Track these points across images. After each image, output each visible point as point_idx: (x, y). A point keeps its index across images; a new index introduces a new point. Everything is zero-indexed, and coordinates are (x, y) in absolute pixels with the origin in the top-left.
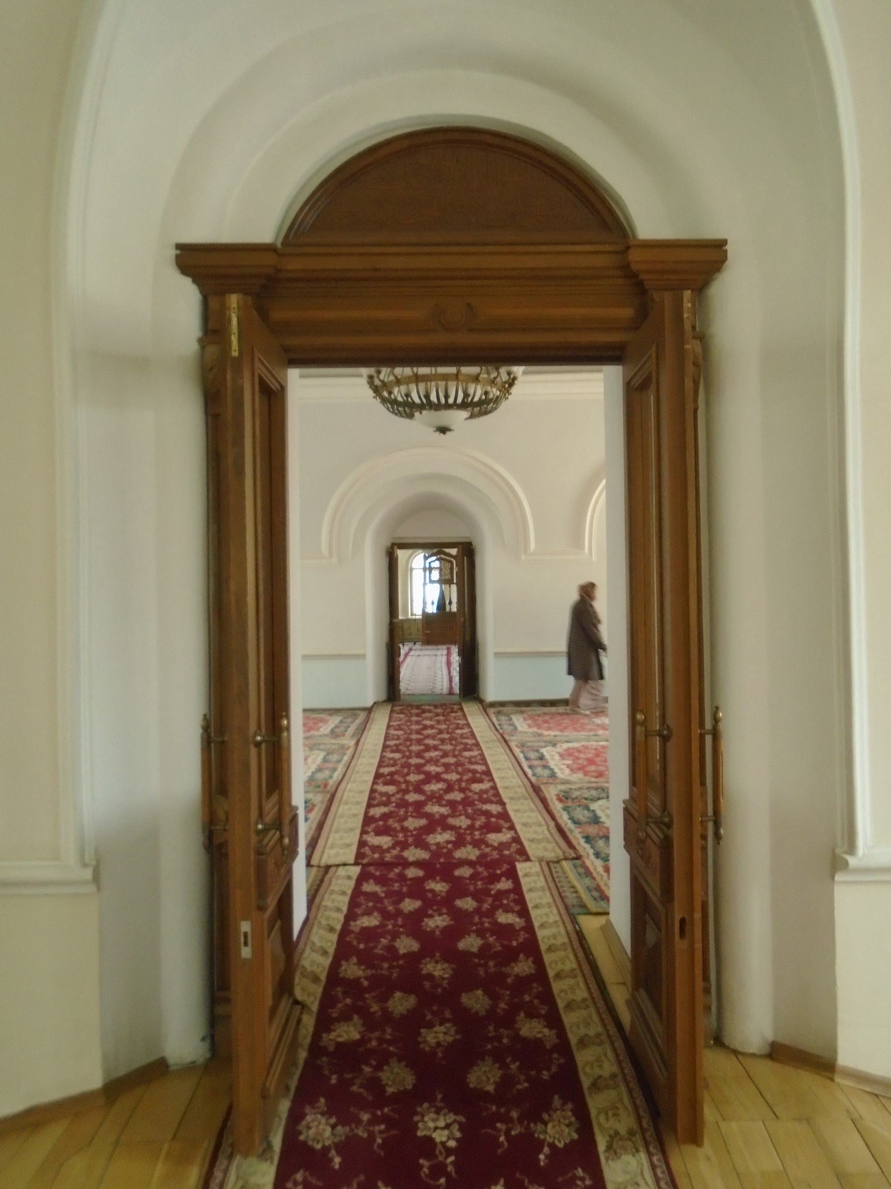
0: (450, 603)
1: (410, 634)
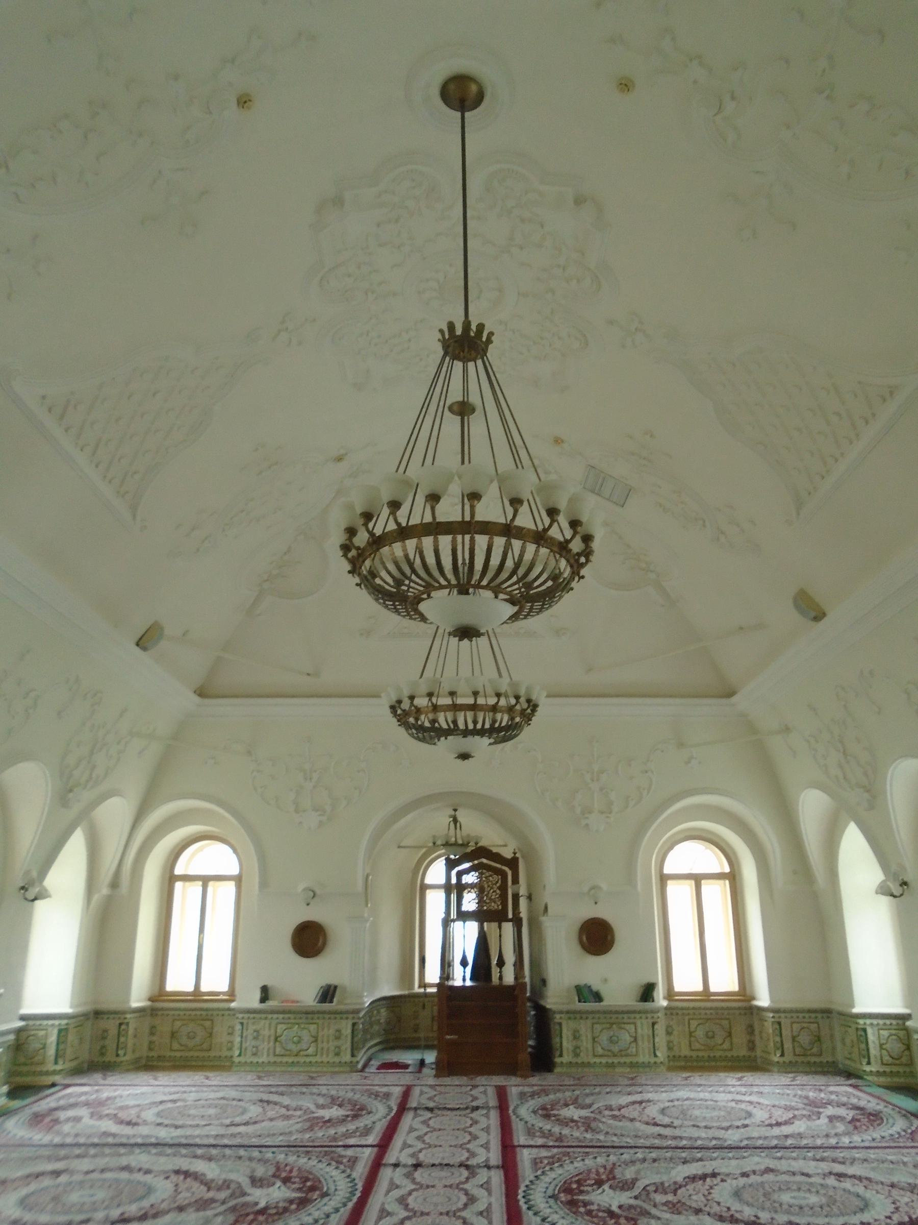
0: (501, 963)
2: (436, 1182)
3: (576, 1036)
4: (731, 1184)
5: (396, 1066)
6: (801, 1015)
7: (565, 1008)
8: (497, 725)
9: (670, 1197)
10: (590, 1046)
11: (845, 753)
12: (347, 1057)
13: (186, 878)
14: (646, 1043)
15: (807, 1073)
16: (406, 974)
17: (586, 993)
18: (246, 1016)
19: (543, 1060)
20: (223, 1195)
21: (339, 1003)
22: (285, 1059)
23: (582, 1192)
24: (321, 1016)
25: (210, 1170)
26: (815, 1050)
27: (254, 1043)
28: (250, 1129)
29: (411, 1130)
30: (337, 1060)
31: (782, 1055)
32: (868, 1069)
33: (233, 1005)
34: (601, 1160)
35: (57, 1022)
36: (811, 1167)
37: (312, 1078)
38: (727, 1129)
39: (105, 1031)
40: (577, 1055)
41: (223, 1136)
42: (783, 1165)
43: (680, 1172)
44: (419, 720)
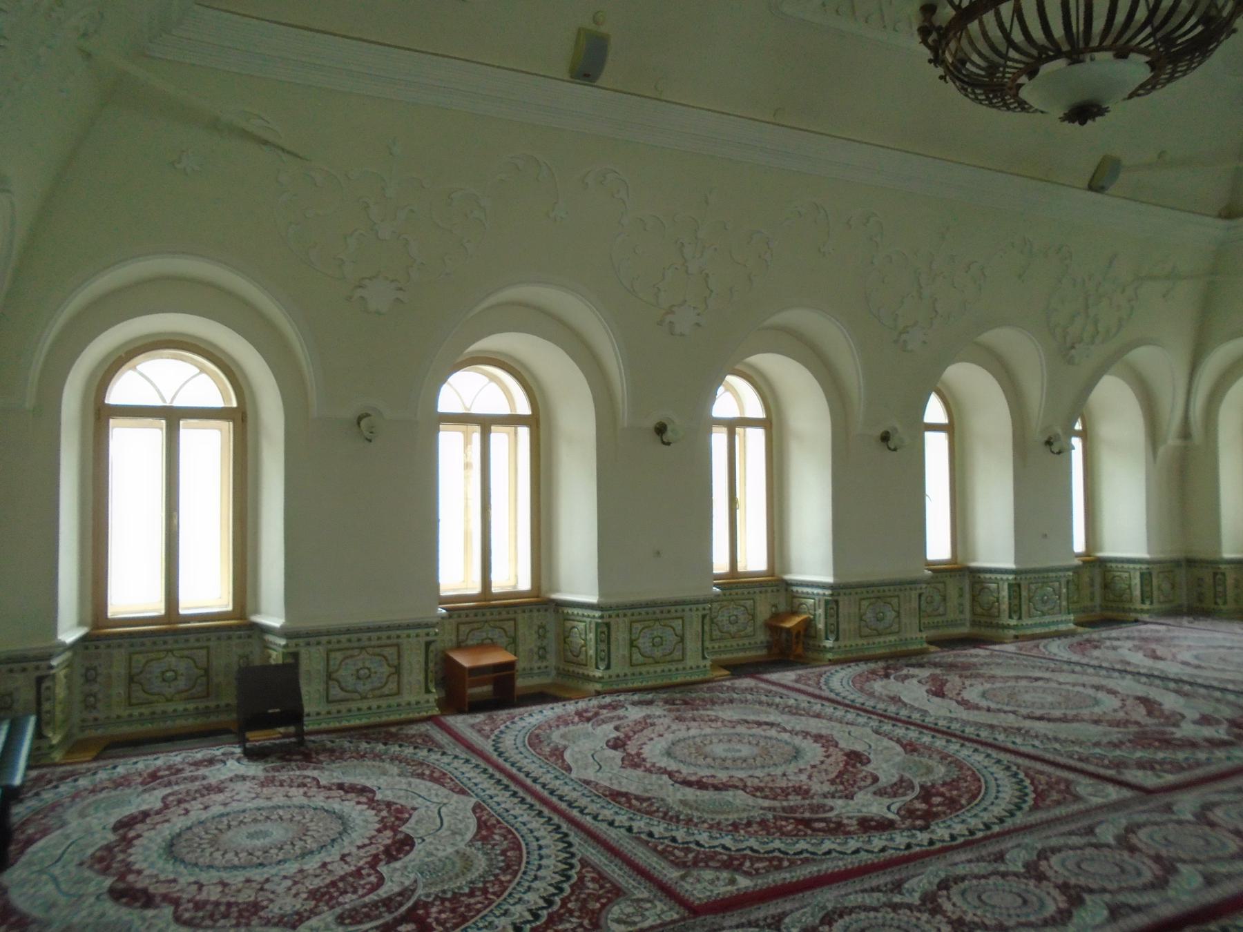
25: (1170, 702)
35: (1138, 566)
39: (1201, 579)
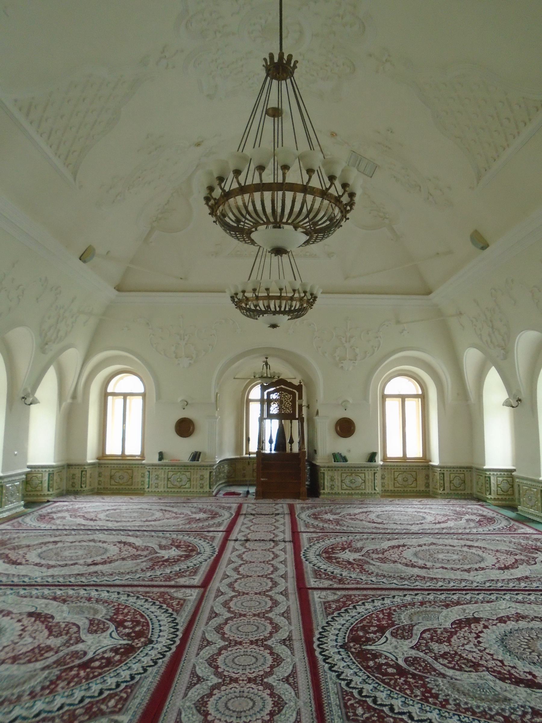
0: (291, 442)
1: (244, 476)
2: (257, 548)
3: (332, 480)
4: (412, 550)
5: (234, 494)
6: (455, 470)
7: (327, 465)
8: (293, 309)
9: (380, 556)
10: (339, 484)
11: (492, 327)
12: (207, 489)
13: (114, 394)
14: (370, 483)
15: (456, 499)
16: (238, 447)
17: (338, 457)
18: (151, 467)
19: (314, 491)
20: (145, 553)
21: (202, 461)
22: (173, 490)
23: (334, 553)
24: (192, 468)
25: (138, 542)
26: (461, 488)
27: (156, 481)
28: (157, 523)
29: (243, 524)
30: (202, 490)
31: (444, 490)
32: (489, 497)
33: (144, 462)
34: (344, 539)
35: (47, 470)
36: (455, 542)
37: (188, 499)
38: (412, 525)
39: (74, 475)
40: (332, 489)
41: (142, 526)
42: (441, 542)
43: (386, 545)
44: (249, 305)
